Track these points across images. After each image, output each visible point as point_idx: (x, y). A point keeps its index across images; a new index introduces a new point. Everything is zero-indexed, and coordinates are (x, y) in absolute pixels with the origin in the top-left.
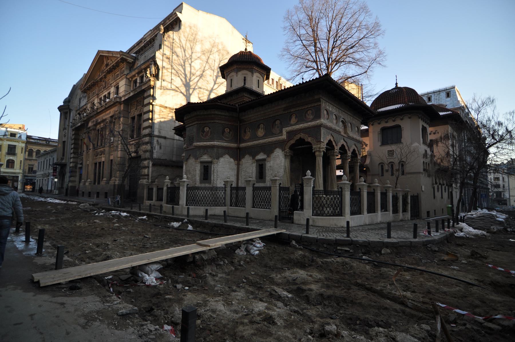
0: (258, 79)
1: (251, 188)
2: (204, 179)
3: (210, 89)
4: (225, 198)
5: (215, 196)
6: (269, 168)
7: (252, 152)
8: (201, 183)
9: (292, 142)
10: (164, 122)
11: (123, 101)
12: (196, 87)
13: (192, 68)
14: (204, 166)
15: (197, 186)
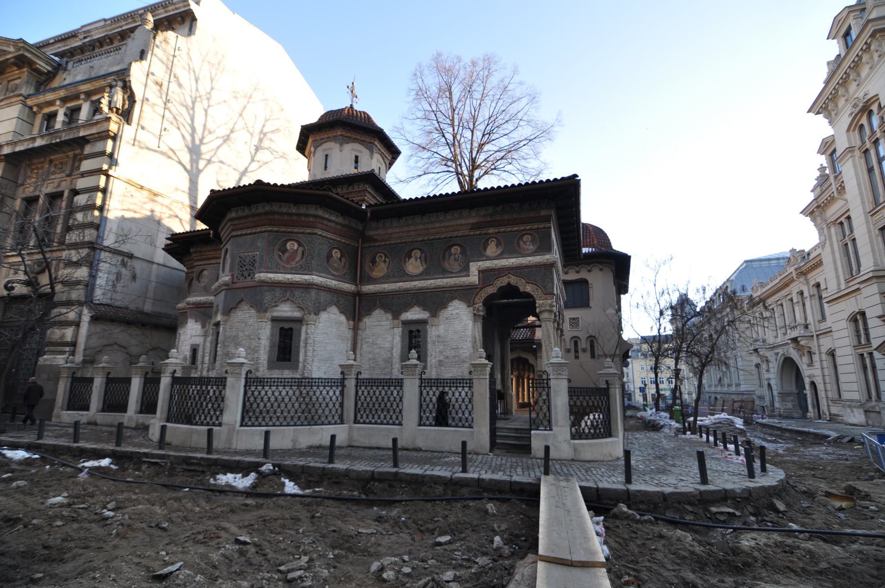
0: (379, 165)
1: (417, 382)
2: (279, 359)
3: (242, 169)
4: (342, 405)
5: (307, 400)
6: (434, 338)
7: (394, 304)
8: (271, 367)
9: (491, 290)
10: (133, 220)
11: (6, 156)
12: (213, 159)
13: (209, 118)
14: (282, 329)
15: (259, 374)
